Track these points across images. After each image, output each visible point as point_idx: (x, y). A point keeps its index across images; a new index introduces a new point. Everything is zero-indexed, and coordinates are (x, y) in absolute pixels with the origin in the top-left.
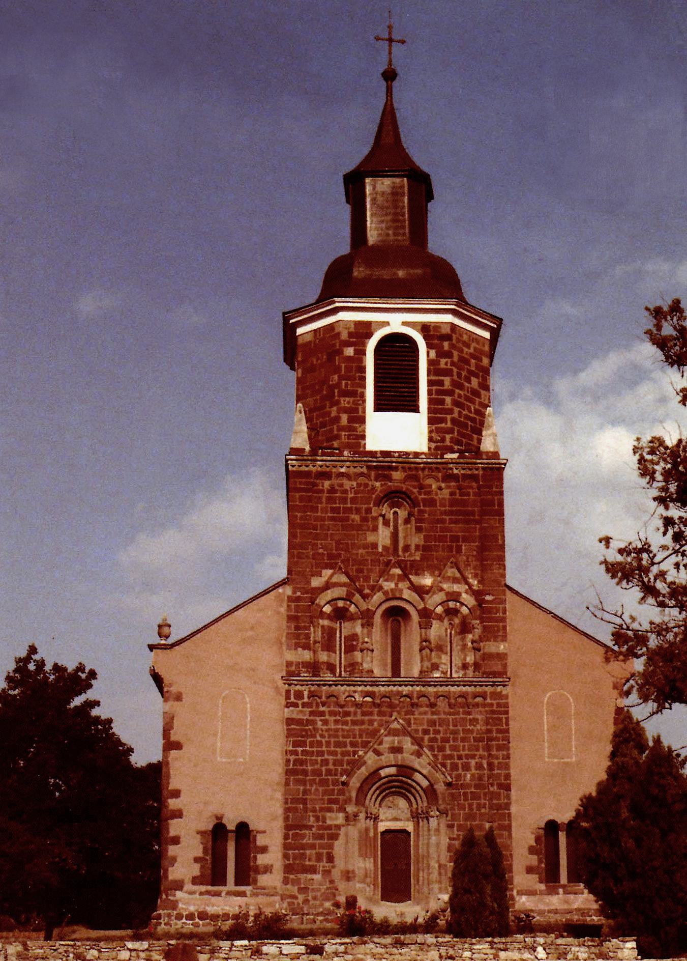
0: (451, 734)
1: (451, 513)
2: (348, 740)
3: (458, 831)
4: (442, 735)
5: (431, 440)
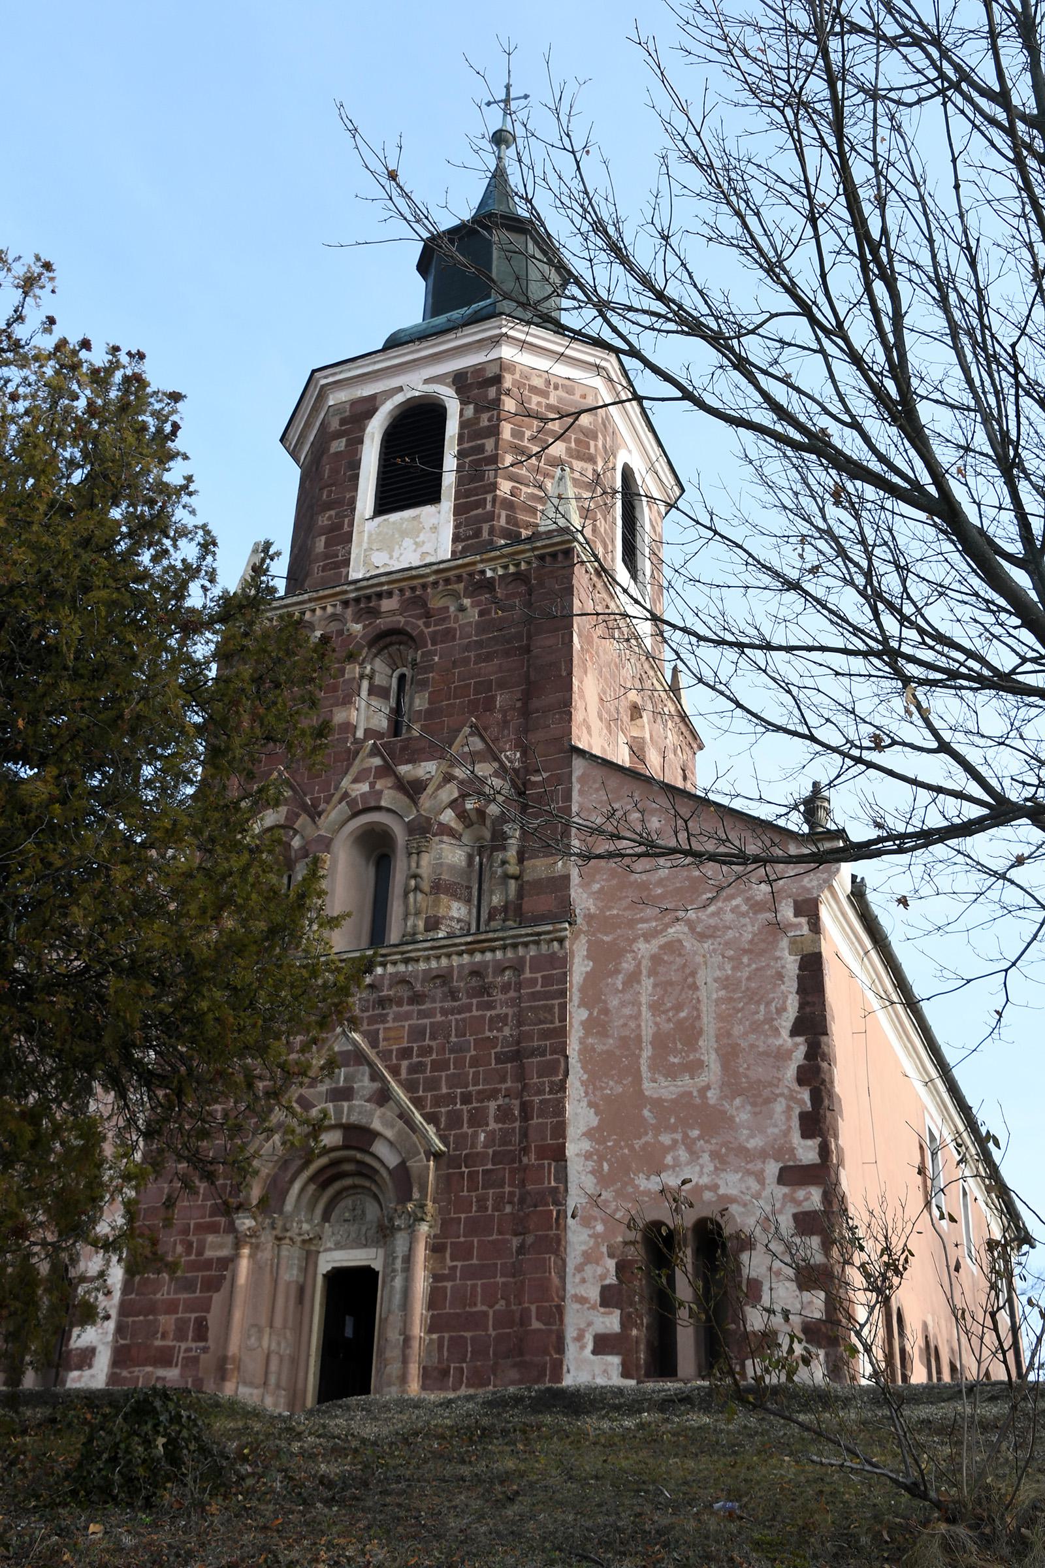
0: (451, 1051)
1: (479, 644)
3: (452, 1260)
4: (434, 1056)
5: (456, 539)
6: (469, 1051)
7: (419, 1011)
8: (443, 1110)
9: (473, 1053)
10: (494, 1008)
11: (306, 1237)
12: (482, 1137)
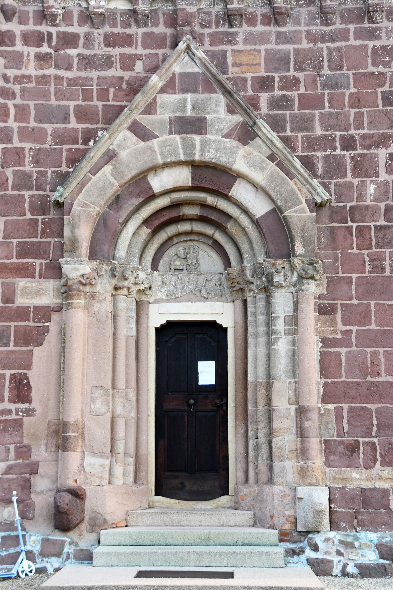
0: (325, 86)
2: (72, 104)
3: (345, 323)
4: (302, 90)
6: (348, 87)
7: (278, 34)
8: (319, 154)
9: (353, 90)
10: (379, 37)
11: (142, 287)
12: (371, 189)
